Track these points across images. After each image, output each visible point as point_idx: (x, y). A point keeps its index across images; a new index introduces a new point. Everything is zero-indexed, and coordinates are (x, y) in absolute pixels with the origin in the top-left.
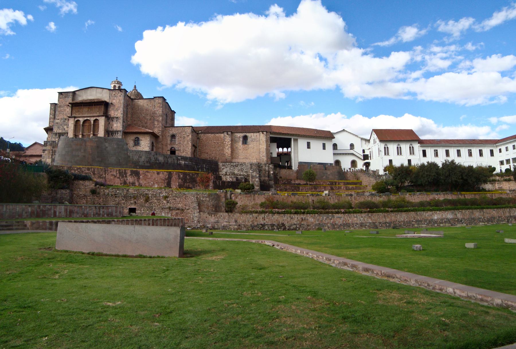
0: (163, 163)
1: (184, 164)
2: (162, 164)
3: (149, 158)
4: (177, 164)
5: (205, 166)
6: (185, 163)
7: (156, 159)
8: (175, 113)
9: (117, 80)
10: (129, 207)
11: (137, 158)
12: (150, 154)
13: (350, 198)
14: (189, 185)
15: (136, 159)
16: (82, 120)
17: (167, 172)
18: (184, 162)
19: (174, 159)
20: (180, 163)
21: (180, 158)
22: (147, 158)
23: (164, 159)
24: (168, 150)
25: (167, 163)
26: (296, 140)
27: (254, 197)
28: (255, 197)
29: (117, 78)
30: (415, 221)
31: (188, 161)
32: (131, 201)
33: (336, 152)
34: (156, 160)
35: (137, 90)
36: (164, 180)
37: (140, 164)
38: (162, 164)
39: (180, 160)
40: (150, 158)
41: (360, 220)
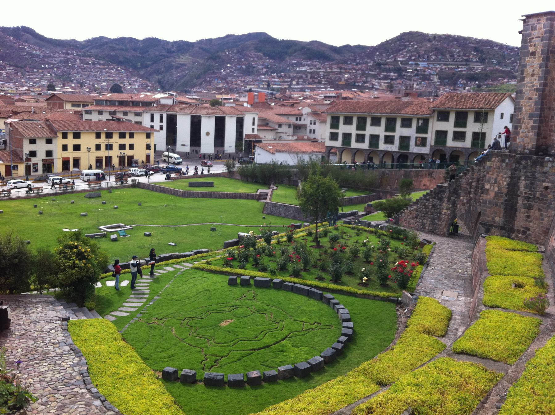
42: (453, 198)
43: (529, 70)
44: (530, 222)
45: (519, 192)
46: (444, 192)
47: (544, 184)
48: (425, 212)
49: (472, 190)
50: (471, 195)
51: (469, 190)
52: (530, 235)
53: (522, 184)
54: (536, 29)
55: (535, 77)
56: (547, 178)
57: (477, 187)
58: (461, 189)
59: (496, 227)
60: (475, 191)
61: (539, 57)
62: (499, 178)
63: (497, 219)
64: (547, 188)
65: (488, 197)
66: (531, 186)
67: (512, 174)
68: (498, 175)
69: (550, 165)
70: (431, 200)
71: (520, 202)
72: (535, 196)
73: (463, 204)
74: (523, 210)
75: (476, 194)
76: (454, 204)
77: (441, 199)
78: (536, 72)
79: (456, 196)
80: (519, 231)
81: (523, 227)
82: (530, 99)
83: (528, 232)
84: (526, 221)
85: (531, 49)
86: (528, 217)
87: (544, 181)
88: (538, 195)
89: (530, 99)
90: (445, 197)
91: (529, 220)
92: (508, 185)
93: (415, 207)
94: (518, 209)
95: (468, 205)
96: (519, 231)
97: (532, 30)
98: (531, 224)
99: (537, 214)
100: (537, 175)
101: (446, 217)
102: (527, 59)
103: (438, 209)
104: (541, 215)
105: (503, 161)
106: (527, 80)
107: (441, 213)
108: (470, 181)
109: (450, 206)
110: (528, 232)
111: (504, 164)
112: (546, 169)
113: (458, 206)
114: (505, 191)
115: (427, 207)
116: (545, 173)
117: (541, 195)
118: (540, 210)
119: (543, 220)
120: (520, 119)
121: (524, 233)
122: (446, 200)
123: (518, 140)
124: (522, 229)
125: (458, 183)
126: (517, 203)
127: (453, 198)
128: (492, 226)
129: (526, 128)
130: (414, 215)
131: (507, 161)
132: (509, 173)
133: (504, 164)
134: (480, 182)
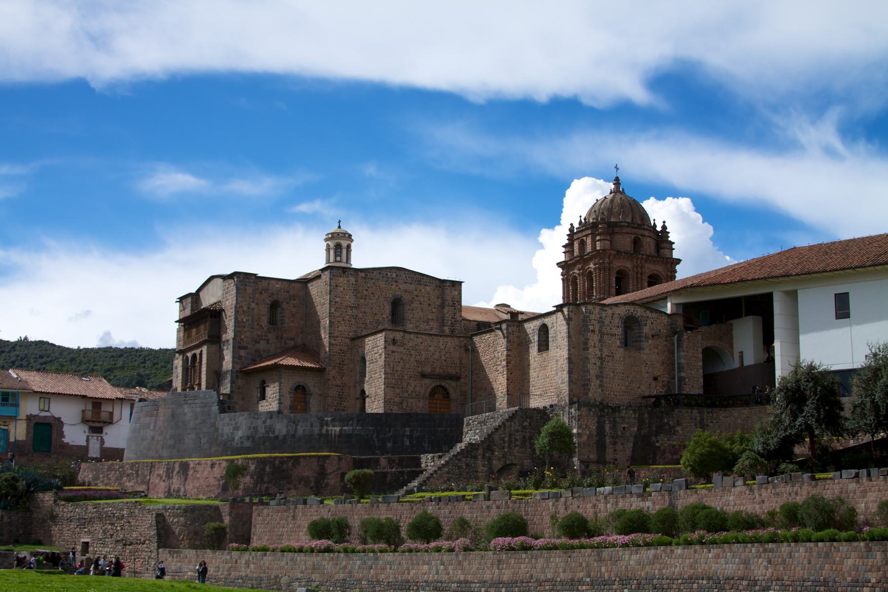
0: (285, 436)
1: (337, 433)
2: (281, 438)
3: (254, 428)
4: (320, 435)
5: (411, 431)
6: (341, 431)
7: (270, 429)
8: (460, 283)
9: (339, 227)
10: (83, 540)
11: (231, 431)
12: (258, 419)
13: (553, 505)
14: (267, 488)
15: (227, 435)
16: (189, 355)
17: (227, 460)
18: (338, 429)
19: (312, 425)
20: (327, 431)
21: (329, 419)
22: (250, 429)
23: (287, 427)
24: (357, 399)
25: (293, 436)
26: (793, 296)
27: (294, 512)
28: (297, 511)
29: (339, 222)
30: (588, 580)
31: (352, 425)
32: (85, 528)
33: (132, 402)
34: (268, 433)
35: (623, 193)
36: (219, 480)
37: (235, 444)
38: (281, 438)
39: (327, 425)
40: (256, 429)
41: (437, 573)
42: (487, 455)
43: (591, 343)
44: (617, 454)
45: (606, 433)
46: (477, 449)
47: (623, 426)
48: (459, 473)
49: (506, 445)
50: (506, 450)
51: (503, 445)
52: (618, 464)
53: (607, 427)
54: (593, 314)
55: (596, 349)
56: (624, 421)
57: (510, 442)
58: (494, 445)
59: (592, 462)
60: (509, 445)
61: (598, 335)
62: (589, 424)
63: (592, 457)
64: (624, 428)
65: (582, 440)
66: (614, 427)
67: (599, 419)
68: (588, 421)
69: (624, 411)
70: (463, 459)
71: (608, 441)
72: (617, 435)
73: (499, 459)
74: (611, 446)
75: (510, 448)
76: (490, 460)
77: (475, 457)
78: (597, 345)
79: (490, 452)
80: (610, 463)
81: (612, 459)
82: (595, 364)
83: (616, 462)
84: (614, 454)
85: (591, 328)
86: (615, 450)
87: (622, 423)
88: (619, 433)
89: (595, 364)
90: (479, 455)
91: (616, 453)
92: (596, 428)
93: (446, 469)
94: (607, 446)
95: (504, 459)
96: (610, 463)
97: (590, 314)
98: (618, 456)
99: (621, 448)
100: (617, 420)
101: (484, 474)
102: (589, 334)
103: (473, 467)
104: (624, 447)
105: (590, 410)
106: (591, 350)
107: (477, 472)
108: (503, 436)
109: (486, 463)
110: (616, 462)
111: (592, 413)
112: (623, 415)
113: (494, 461)
114: (595, 433)
115: (460, 468)
116: (622, 417)
117: (622, 433)
118: (622, 444)
119: (625, 451)
120: (589, 379)
121: (614, 463)
122: (480, 457)
123: (590, 395)
124: (612, 461)
125: (491, 439)
126: (605, 441)
127: (487, 455)
128: (589, 462)
129: (595, 385)
130: (446, 479)
131: (593, 410)
132: (596, 419)
133: (592, 413)
134: (513, 437)
